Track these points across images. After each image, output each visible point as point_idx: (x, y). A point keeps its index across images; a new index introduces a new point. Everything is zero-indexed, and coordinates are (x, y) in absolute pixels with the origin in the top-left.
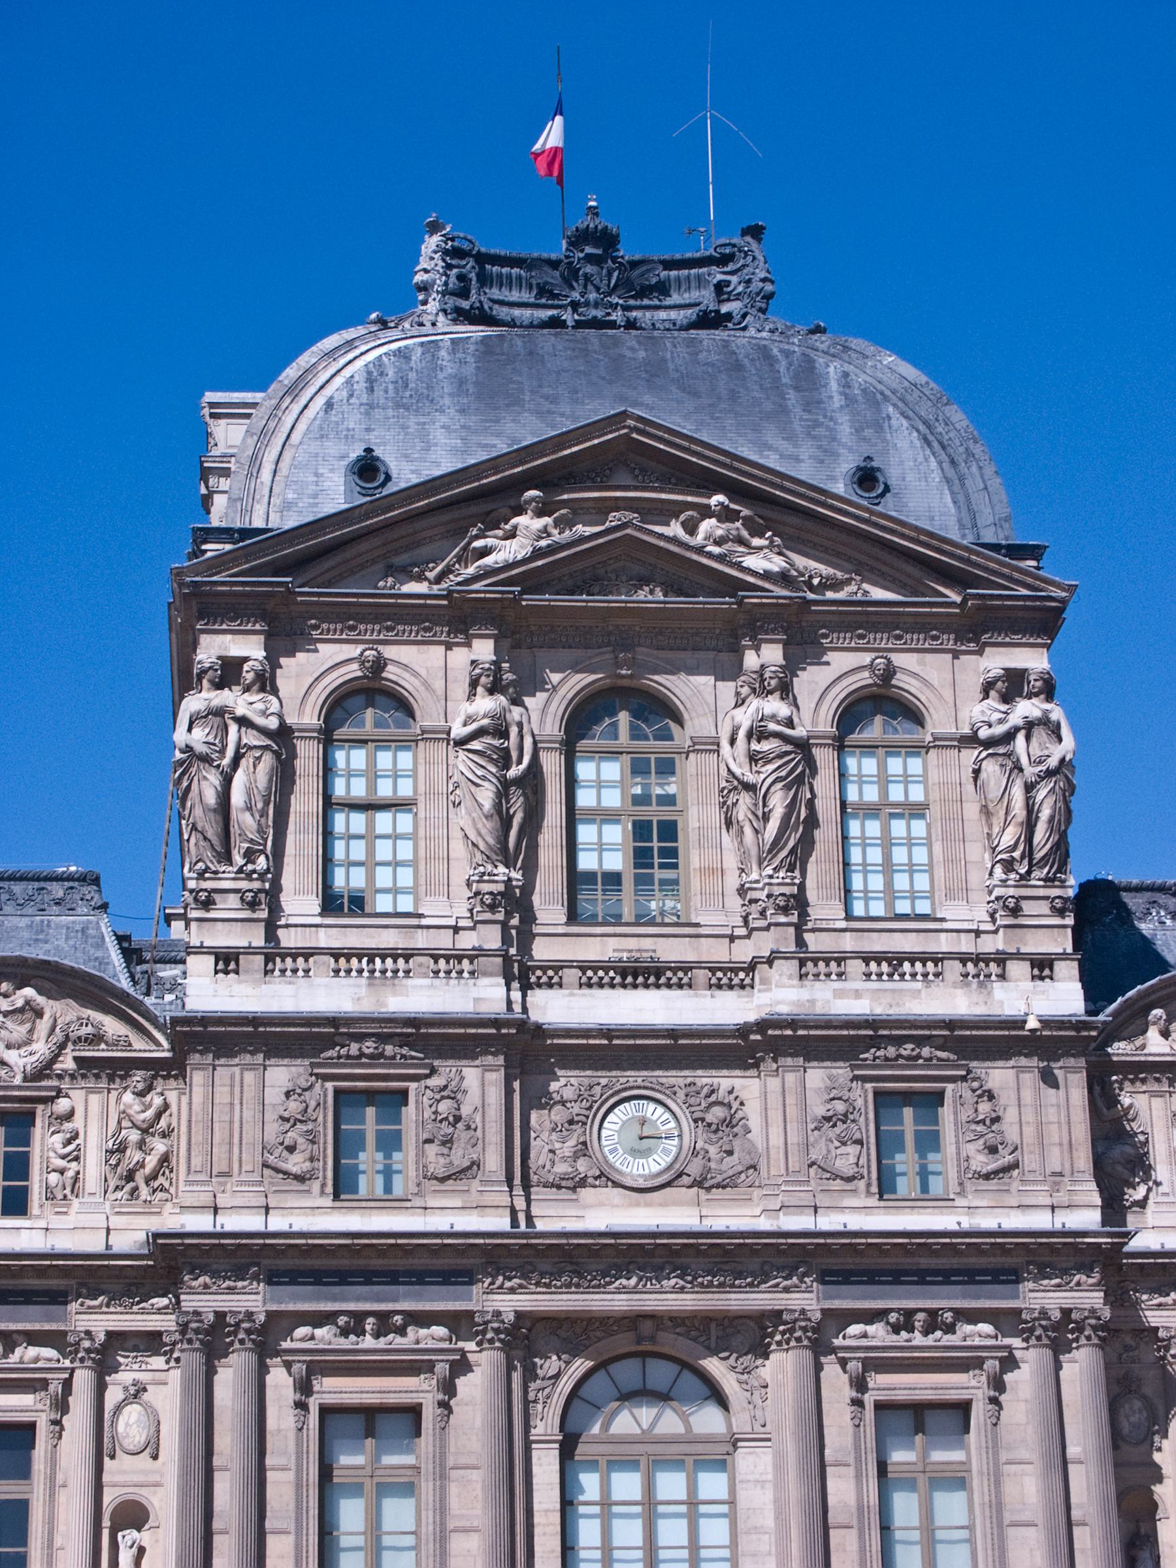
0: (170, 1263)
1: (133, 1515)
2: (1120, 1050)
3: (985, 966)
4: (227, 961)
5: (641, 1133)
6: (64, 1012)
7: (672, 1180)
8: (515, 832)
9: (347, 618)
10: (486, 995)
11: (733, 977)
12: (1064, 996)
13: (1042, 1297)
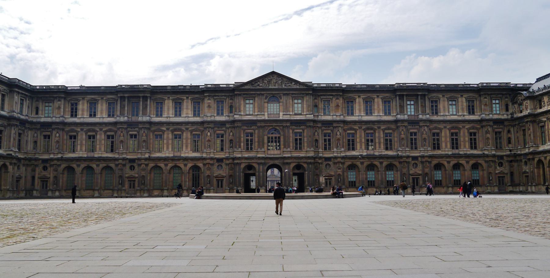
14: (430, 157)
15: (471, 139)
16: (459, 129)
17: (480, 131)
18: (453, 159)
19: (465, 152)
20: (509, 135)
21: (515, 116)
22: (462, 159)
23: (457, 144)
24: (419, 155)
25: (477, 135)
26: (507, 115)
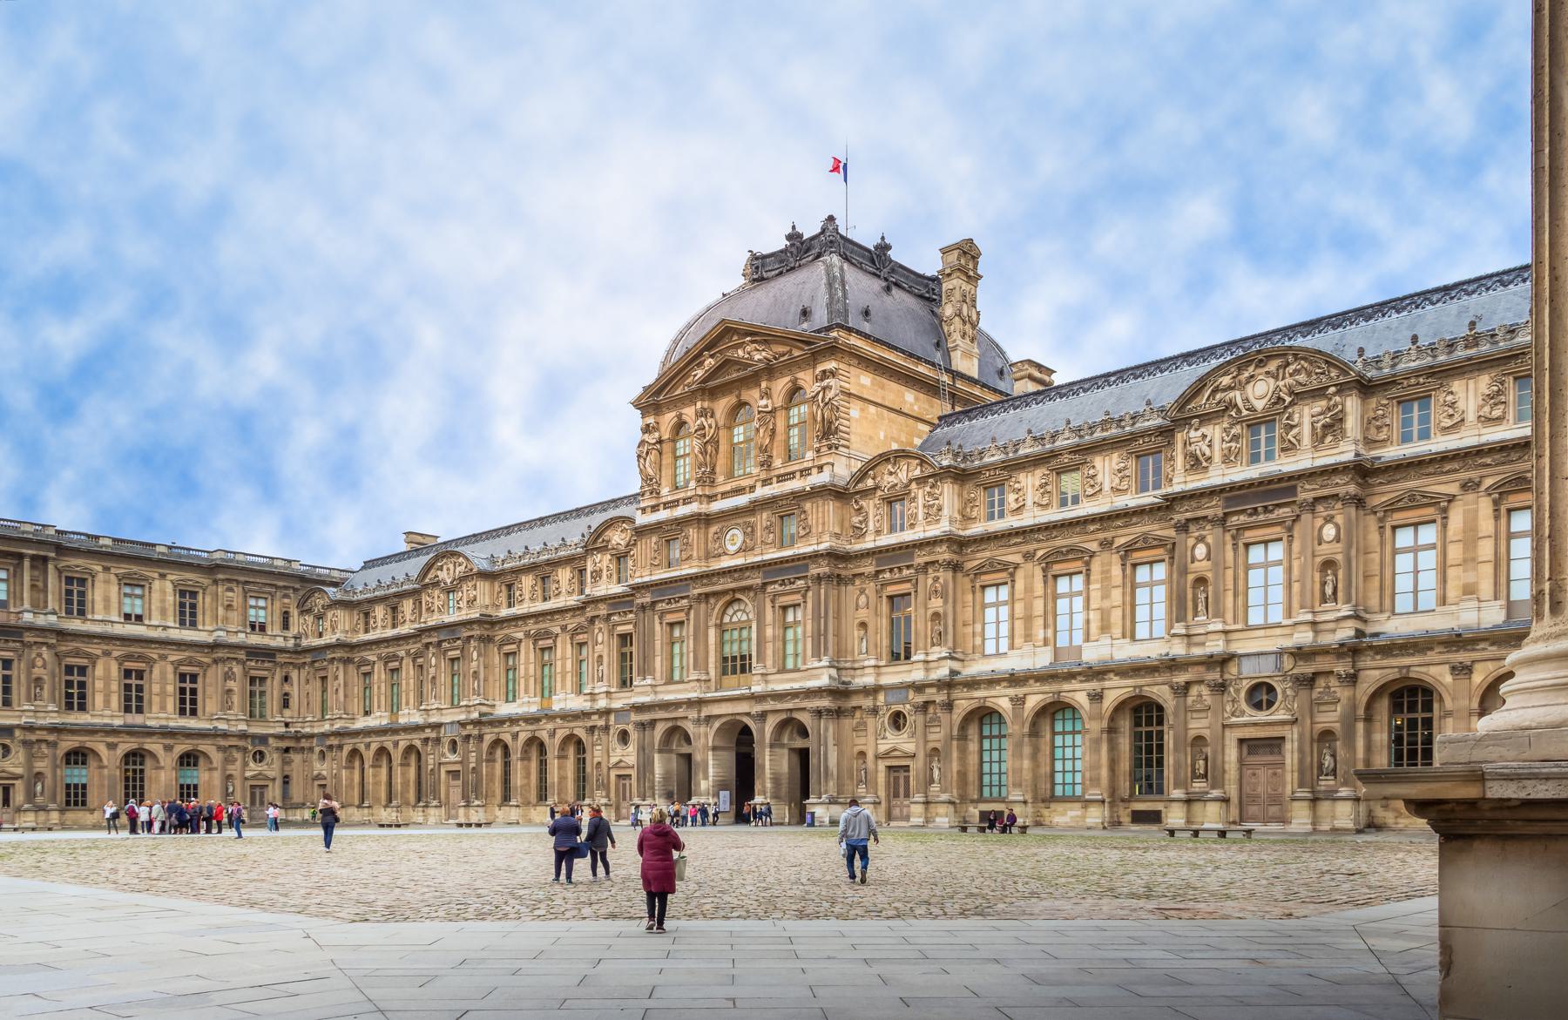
2: (860, 486)
3: (805, 472)
4: (644, 510)
7: (743, 550)
10: (694, 508)
14: (54, 729)
15: (182, 691)
17: (210, 672)
18: (127, 738)
19: (164, 723)
20: (287, 688)
21: (305, 643)
22: (154, 739)
23: (140, 699)
24: (15, 722)
25: (200, 679)
26: (285, 638)
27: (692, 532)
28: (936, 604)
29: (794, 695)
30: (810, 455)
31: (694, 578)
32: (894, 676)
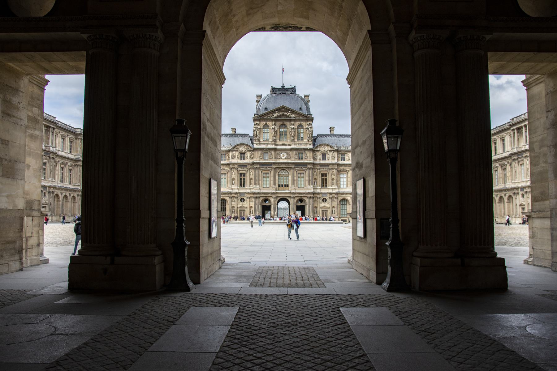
0: (253, 164)
1: (251, 179)
3: (306, 144)
4: (257, 144)
5: (283, 155)
6: (246, 147)
8: (275, 135)
9: (264, 120)
10: (273, 146)
11: (290, 145)
12: (311, 147)
13: (309, 166)
16: (65, 164)
27: (273, 153)
28: (334, 177)
29: (304, 193)
30: (305, 140)
31: (274, 163)
32: (324, 190)
